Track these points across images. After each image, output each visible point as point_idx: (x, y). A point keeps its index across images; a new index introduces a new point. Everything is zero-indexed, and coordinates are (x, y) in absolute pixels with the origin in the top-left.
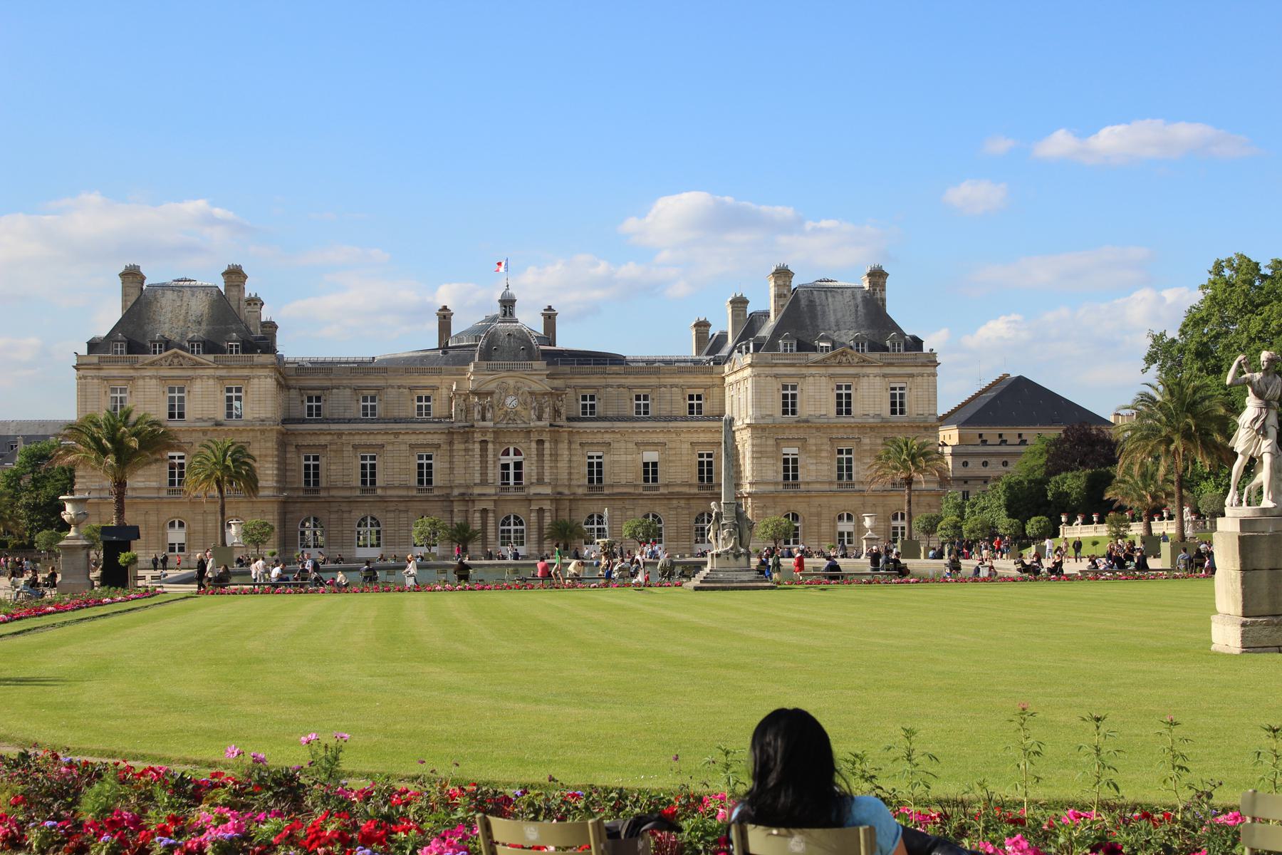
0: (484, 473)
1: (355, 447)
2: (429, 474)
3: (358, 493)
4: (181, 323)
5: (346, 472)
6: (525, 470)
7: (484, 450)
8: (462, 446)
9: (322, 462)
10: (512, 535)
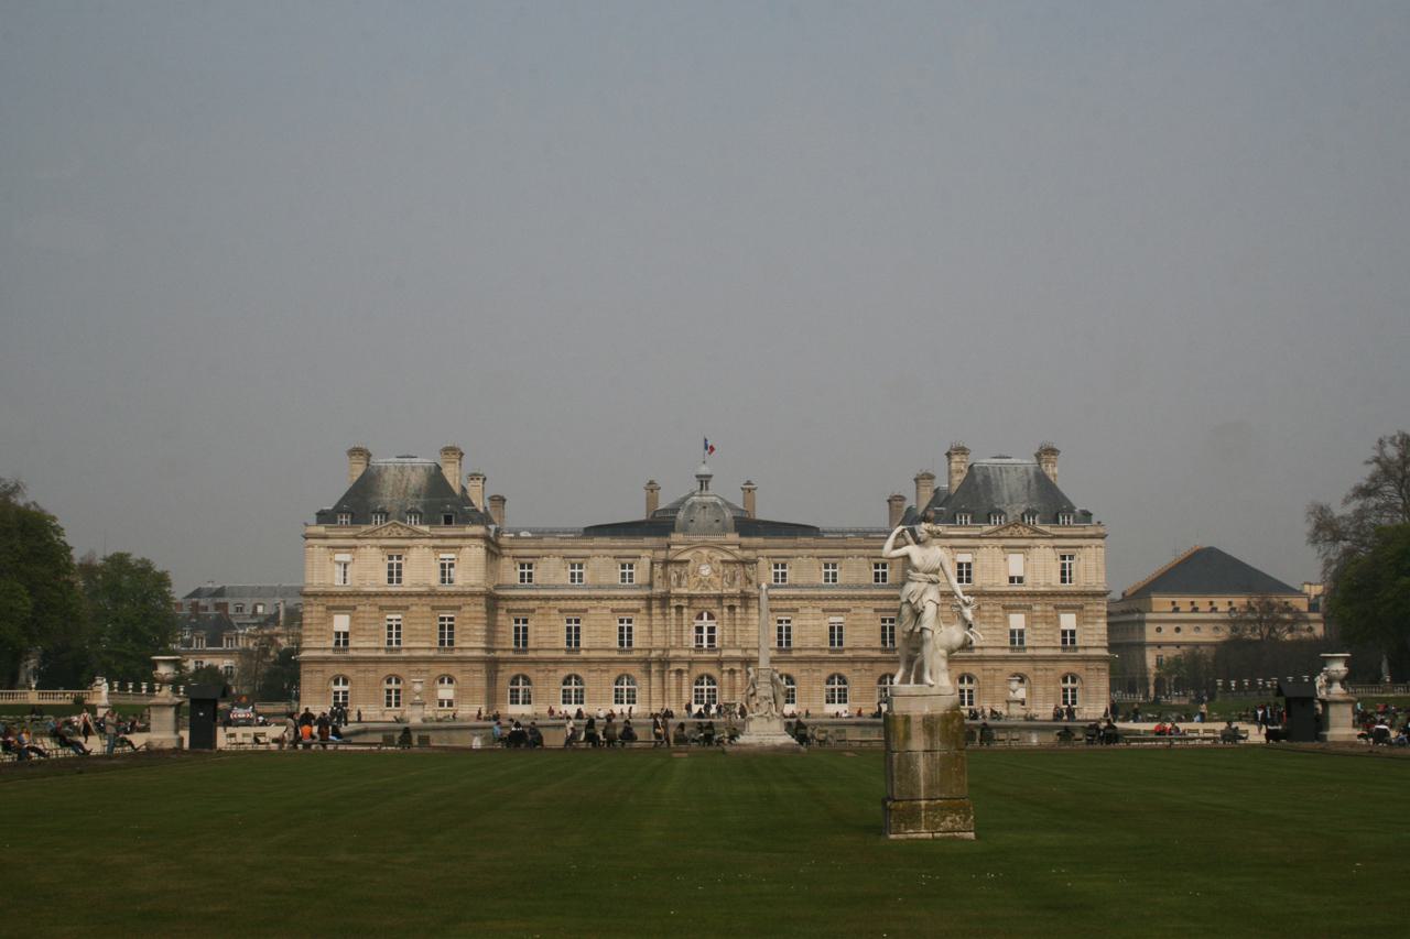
1: (561, 611)
2: (630, 636)
3: (562, 654)
4: (402, 496)
5: (553, 634)
6: (717, 634)
8: (658, 611)
9: (531, 625)
10: (705, 694)
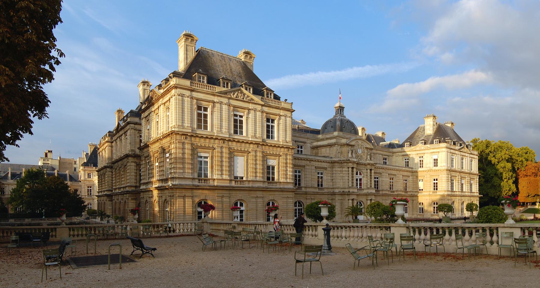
0: (353, 183)
7: (353, 171)
8: (339, 169)
